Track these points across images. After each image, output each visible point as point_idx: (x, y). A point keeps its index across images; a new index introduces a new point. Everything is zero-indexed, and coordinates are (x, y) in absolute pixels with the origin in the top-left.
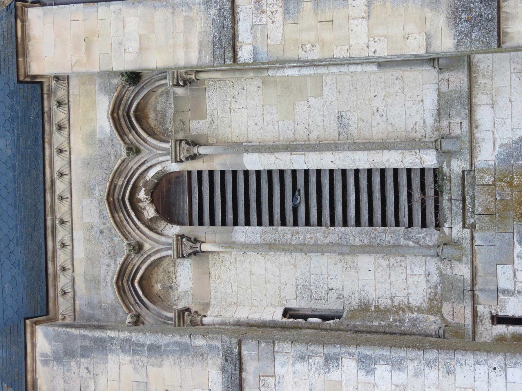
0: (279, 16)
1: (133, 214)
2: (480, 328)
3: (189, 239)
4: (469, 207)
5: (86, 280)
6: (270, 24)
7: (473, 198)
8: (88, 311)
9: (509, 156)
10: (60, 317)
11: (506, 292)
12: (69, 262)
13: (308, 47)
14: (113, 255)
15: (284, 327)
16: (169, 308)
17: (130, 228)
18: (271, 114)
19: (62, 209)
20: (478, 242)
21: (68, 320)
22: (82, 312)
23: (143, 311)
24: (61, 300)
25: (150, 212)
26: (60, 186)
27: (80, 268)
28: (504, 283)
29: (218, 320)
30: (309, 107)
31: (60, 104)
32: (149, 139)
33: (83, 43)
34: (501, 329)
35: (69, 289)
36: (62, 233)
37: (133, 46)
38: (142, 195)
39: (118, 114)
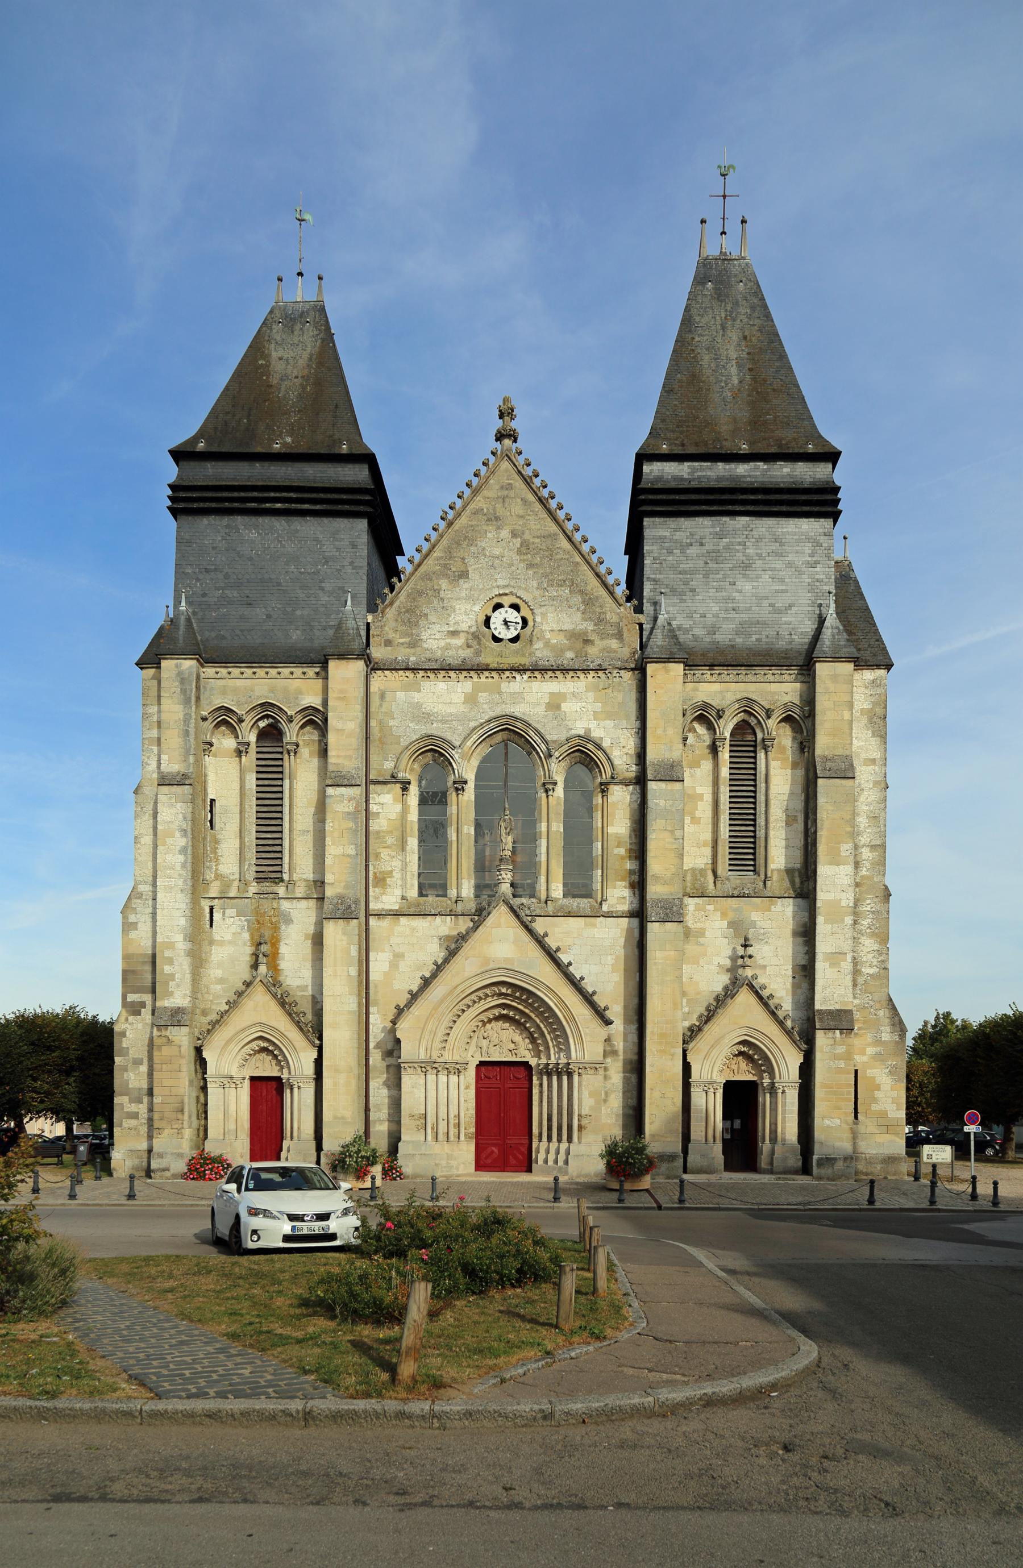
1: (259, 716)
2: (207, 900)
3: (246, 749)
4: (262, 896)
5: (224, 686)
7: (267, 898)
8: (208, 687)
9: (285, 916)
10: (204, 670)
11: (224, 912)
12: (234, 676)
14: (239, 704)
15: (204, 801)
16: (211, 737)
17: (253, 714)
19: (261, 672)
20: (246, 900)
21: (202, 675)
22: (208, 683)
23: (210, 720)
24: (214, 670)
25: (262, 724)
26: (273, 672)
27: (231, 683)
28: (228, 912)
29: (207, 764)
31: (317, 673)
34: (207, 910)
35: (219, 676)
36: (248, 672)
38: (271, 720)
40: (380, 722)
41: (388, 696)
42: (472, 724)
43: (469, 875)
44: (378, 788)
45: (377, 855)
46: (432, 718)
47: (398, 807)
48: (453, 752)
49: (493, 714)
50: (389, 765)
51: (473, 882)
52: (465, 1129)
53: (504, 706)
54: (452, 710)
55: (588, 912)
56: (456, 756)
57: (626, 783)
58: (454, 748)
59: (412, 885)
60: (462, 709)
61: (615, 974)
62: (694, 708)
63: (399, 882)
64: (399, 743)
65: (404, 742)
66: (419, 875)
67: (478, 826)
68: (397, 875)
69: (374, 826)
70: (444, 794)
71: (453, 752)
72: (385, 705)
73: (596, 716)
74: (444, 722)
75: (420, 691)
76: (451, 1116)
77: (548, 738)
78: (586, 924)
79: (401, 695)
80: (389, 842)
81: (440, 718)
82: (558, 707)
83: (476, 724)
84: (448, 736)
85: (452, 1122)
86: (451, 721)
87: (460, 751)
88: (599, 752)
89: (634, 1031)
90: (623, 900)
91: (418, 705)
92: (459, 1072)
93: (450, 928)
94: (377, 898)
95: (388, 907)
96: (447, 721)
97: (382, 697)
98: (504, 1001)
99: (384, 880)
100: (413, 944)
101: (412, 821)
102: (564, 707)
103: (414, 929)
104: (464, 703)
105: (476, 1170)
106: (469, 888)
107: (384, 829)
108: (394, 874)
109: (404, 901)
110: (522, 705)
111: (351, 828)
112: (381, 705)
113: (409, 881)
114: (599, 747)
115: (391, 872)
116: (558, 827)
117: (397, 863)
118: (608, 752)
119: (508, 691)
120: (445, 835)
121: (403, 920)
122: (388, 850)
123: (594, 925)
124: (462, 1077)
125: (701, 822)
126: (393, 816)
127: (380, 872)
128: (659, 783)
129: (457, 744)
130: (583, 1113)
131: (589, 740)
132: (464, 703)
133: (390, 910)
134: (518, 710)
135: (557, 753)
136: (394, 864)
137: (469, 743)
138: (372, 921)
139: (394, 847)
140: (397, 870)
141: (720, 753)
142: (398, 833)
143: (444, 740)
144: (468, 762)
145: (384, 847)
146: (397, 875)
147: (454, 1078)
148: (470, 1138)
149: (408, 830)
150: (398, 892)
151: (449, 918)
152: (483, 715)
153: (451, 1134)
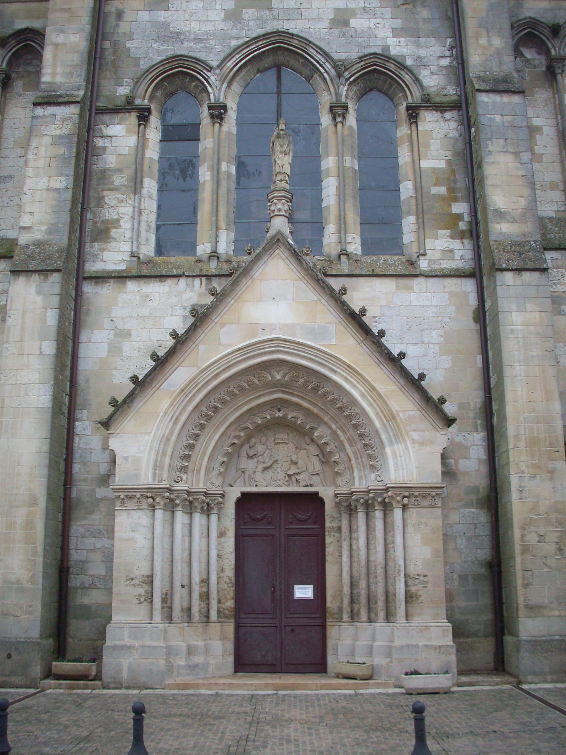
0: (58, 132)
6: (54, 126)
13: (35, 152)
18: (19, 134)
30: (20, 157)
32: (10, 54)
33: (68, 7)
37: (61, 39)
39: (28, 33)
40: (115, 44)
41: (128, 17)
42: (235, 43)
43: (228, 225)
44: (106, 118)
45: (100, 201)
46: (182, 37)
47: (132, 140)
48: (209, 74)
49: (261, 32)
50: (123, 91)
51: (232, 235)
52: (219, 602)
53: (276, 22)
54: (210, 27)
55: (400, 270)
56: (213, 79)
57: (440, 108)
58: (210, 69)
59: (147, 240)
60: (221, 26)
61: (445, 358)
62: (520, 26)
63: (128, 234)
64: (137, 65)
65: (144, 65)
66: (158, 227)
67: (241, 166)
68: (126, 224)
69: (98, 165)
70: (196, 126)
71: (209, 74)
72: (122, 24)
73: (396, 32)
74: (197, 40)
75: (168, 9)
76: (196, 579)
77: (335, 56)
78: (398, 288)
79: (144, 16)
80: (117, 183)
81: (192, 37)
82: (346, 23)
83: (241, 42)
84: (202, 56)
85: (196, 590)
86: (208, 39)
87: (217, 71)
88: (402, 73)
89: (480, 442)
90: (449, 254)
91: (166, 25)
92: (207, 510)
93: (200, 295)
94: (95, 257)
95: (111, 267)
96: (202, 40)
97: (120, 15)
98: (280, 395)
99: (107, 231)
100: (144, 317)
101: (151, 159)
102: (354, 23)
103: (147, 296)
104: (223, 21)
105: (236, 671)
106: (228, 242)
107: (111, 166)
108: (122, 223)
109: (135, 259)
110: (299, 22)
111: (63, 157)
112: (117, 25)
113: (143, 234)
114: (403, 67)
115: (118, 220)
116: (352, 162)
117: (126, 210)
118: (415, 72)
119: (281, 6)
120: (194, 175)
121: (131, 285)
122: (114, 192)
123: (410, 289)
124: (214, 518)
125: (544, 160)
126: (126, 151)
127: (103, 222)
128: (491, 95)
129: (215, 64)
130: (412, 570)
131: (389, 58)
132: (223, 21)
133: (112, 272)
134: (293, 27)
135: (346, 74)
136: (123, 210)
137: (230, 64)
138: (88, 288)
139: (123, 189)
140: (127, 218)
141: (559, 77)
142: (129, 172)
143: (197, 61)
144: (229, 86)
145: (110, 190)
146: (126, 224)
147: (198, 519)
148: (226, 617)
149: (146, 168)
150: (126, 247)
151: (197, 281)
152: (249, 33)
153: (195, 610)
